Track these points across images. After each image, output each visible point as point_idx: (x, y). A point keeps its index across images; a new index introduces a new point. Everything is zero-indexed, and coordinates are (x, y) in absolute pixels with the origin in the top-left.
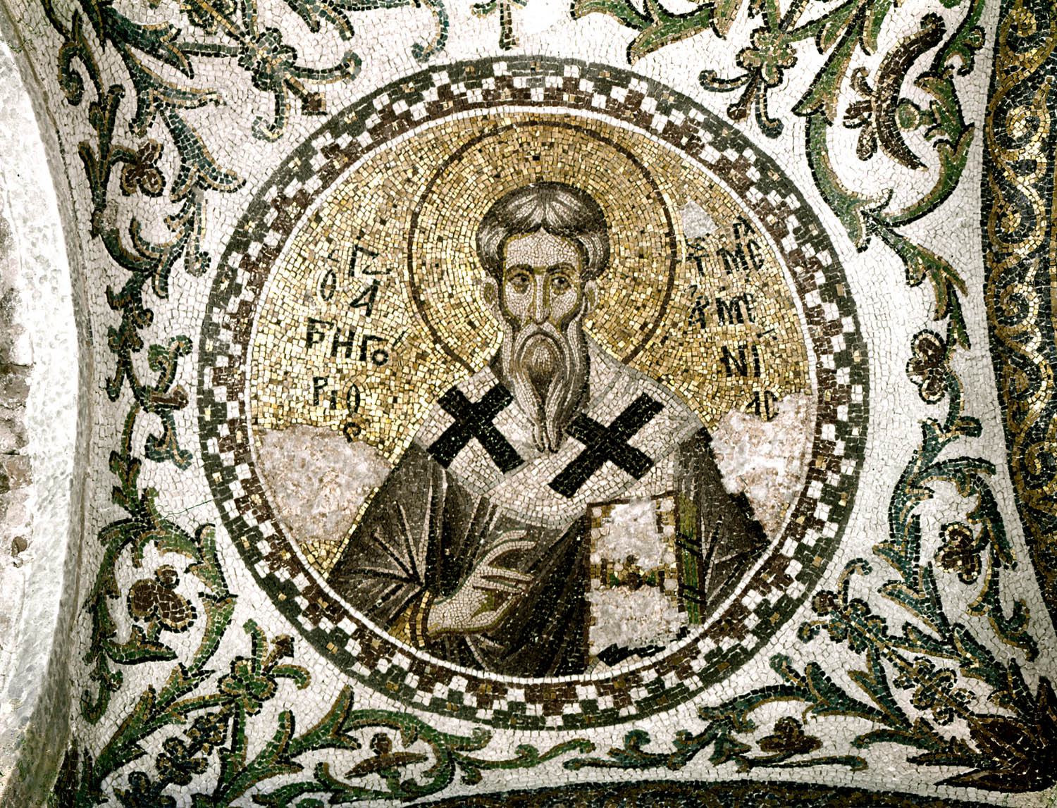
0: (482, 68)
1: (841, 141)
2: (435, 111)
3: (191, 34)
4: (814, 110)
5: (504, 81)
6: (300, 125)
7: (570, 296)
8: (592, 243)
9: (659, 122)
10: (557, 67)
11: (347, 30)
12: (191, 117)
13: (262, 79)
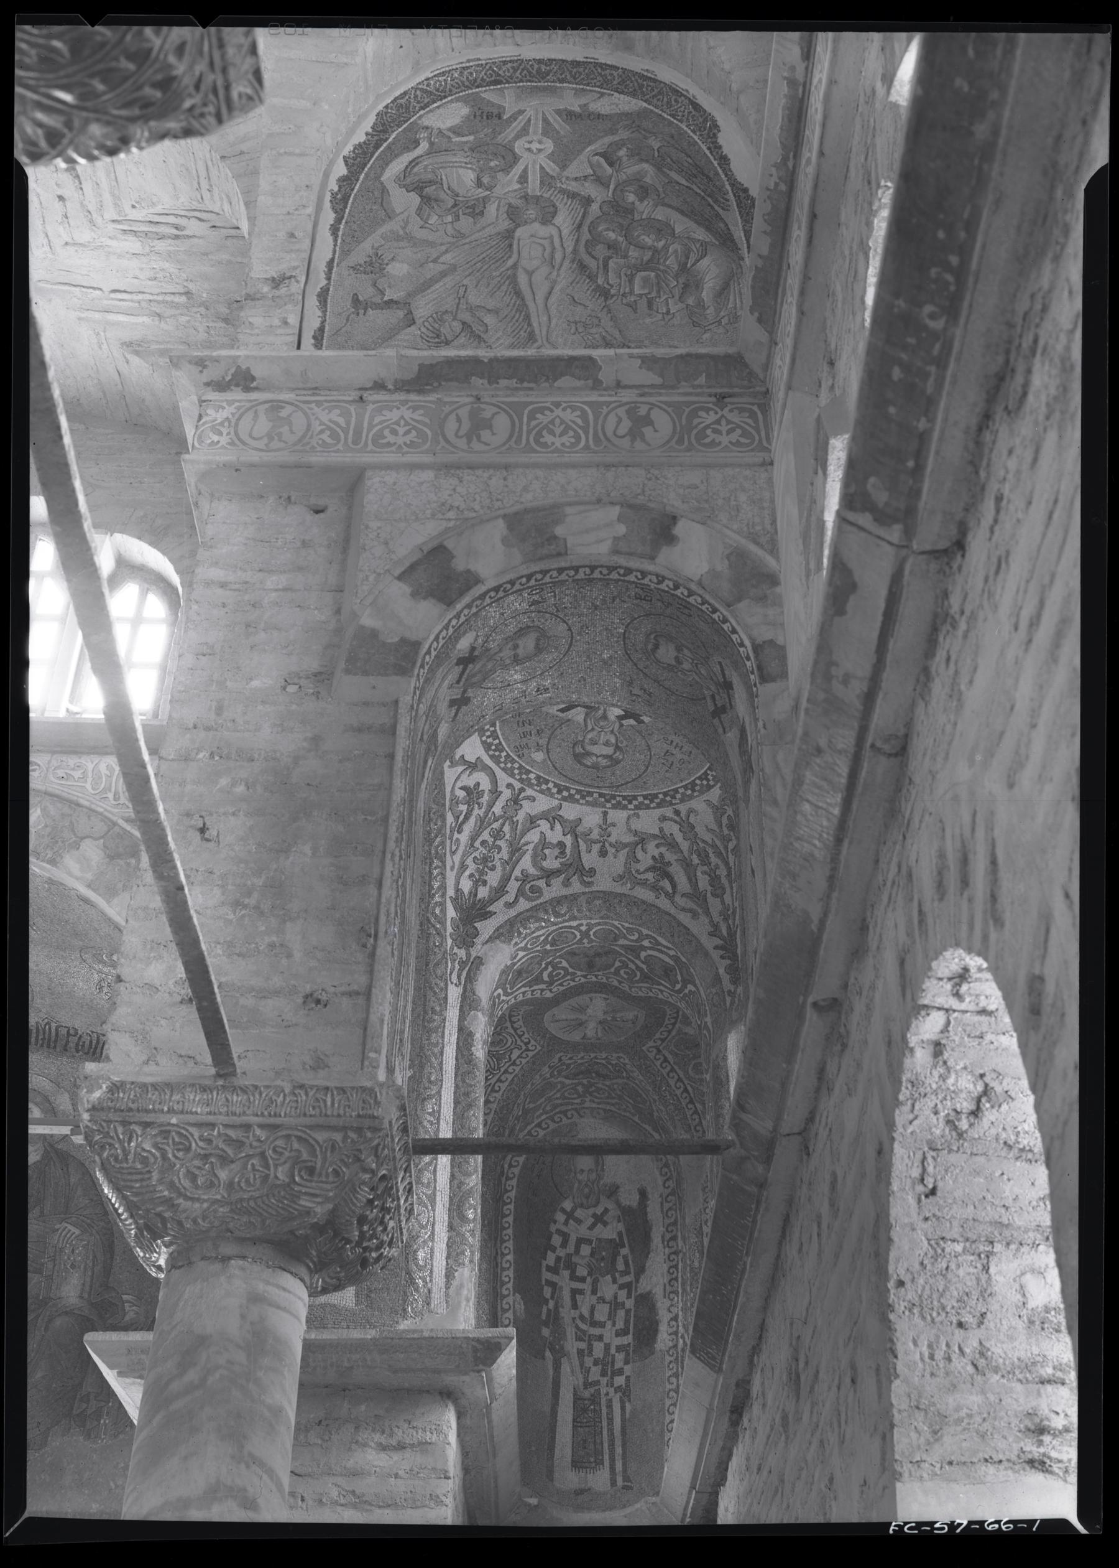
0: (614, 807)
1: (485, 784)
2: (635, 798)
3: (710, 851)
4: (495, 793)
5: (608, 801)
6: (683, 808)
7: (590, 736)
8: (579, 750)
9: (551, 785)
10: (588, 803)
11: (661, 829)
12: (716, 828)
13: (693, 827)
